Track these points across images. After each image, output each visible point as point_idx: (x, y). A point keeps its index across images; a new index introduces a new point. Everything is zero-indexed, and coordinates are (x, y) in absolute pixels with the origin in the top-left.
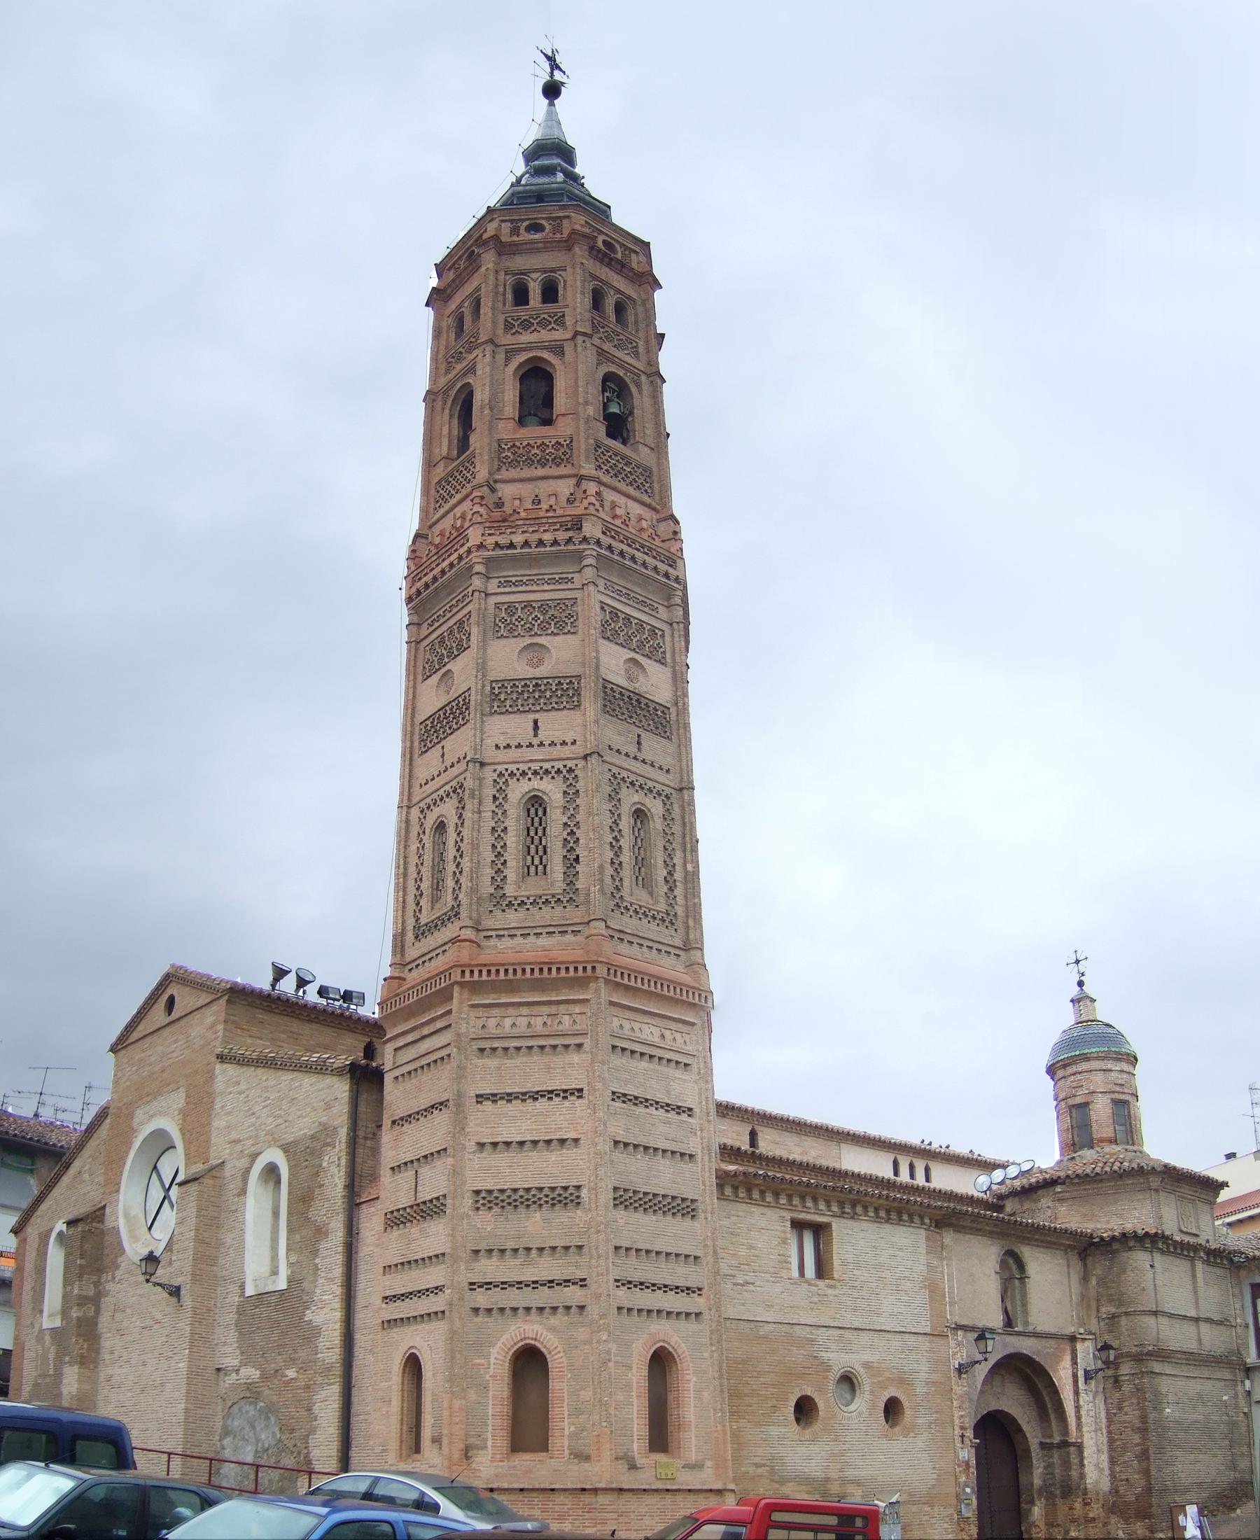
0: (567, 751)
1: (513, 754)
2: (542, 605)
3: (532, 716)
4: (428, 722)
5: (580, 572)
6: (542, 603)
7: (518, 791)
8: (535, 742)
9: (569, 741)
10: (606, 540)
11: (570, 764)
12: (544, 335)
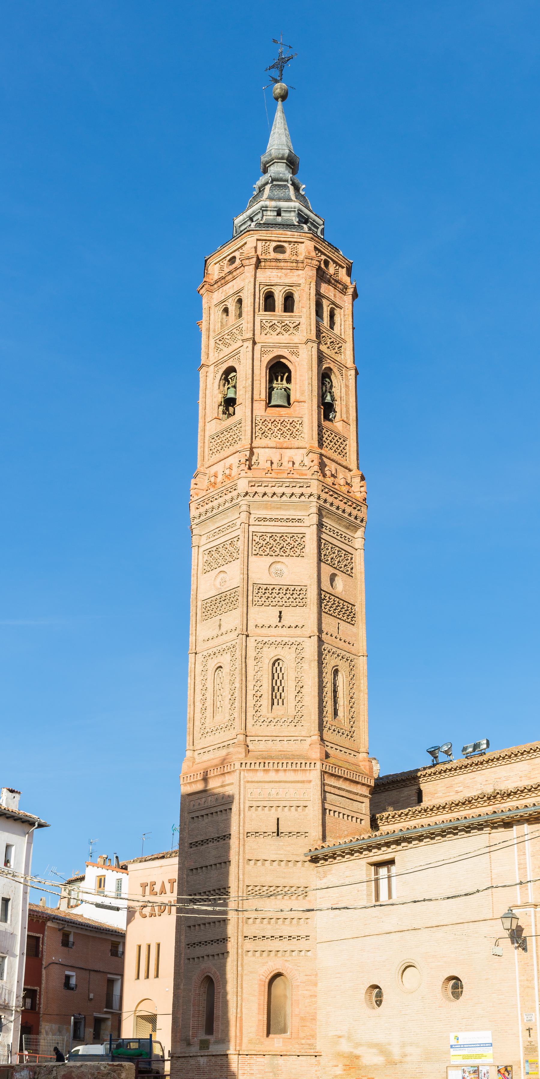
0: (298, 631)
1: (265, 631)
2: (283, 536)
3: (278, 609)
4: (208, 601)
5: (309, 516)
6: (282, 534)
7: (269, 654)
8: (280, 625)
9: (300, 626)
10: (324, 496)
11: (300, 640)
12: (284, 338)
